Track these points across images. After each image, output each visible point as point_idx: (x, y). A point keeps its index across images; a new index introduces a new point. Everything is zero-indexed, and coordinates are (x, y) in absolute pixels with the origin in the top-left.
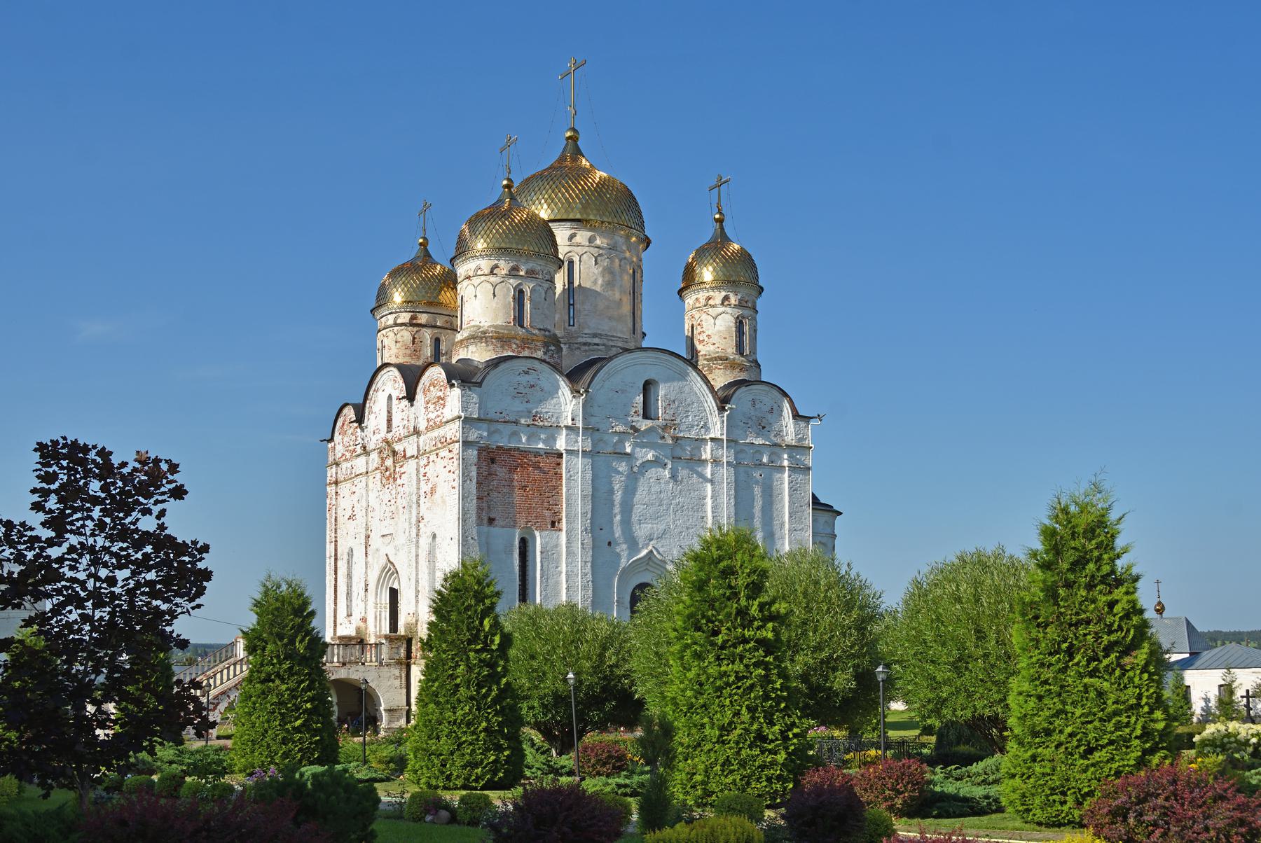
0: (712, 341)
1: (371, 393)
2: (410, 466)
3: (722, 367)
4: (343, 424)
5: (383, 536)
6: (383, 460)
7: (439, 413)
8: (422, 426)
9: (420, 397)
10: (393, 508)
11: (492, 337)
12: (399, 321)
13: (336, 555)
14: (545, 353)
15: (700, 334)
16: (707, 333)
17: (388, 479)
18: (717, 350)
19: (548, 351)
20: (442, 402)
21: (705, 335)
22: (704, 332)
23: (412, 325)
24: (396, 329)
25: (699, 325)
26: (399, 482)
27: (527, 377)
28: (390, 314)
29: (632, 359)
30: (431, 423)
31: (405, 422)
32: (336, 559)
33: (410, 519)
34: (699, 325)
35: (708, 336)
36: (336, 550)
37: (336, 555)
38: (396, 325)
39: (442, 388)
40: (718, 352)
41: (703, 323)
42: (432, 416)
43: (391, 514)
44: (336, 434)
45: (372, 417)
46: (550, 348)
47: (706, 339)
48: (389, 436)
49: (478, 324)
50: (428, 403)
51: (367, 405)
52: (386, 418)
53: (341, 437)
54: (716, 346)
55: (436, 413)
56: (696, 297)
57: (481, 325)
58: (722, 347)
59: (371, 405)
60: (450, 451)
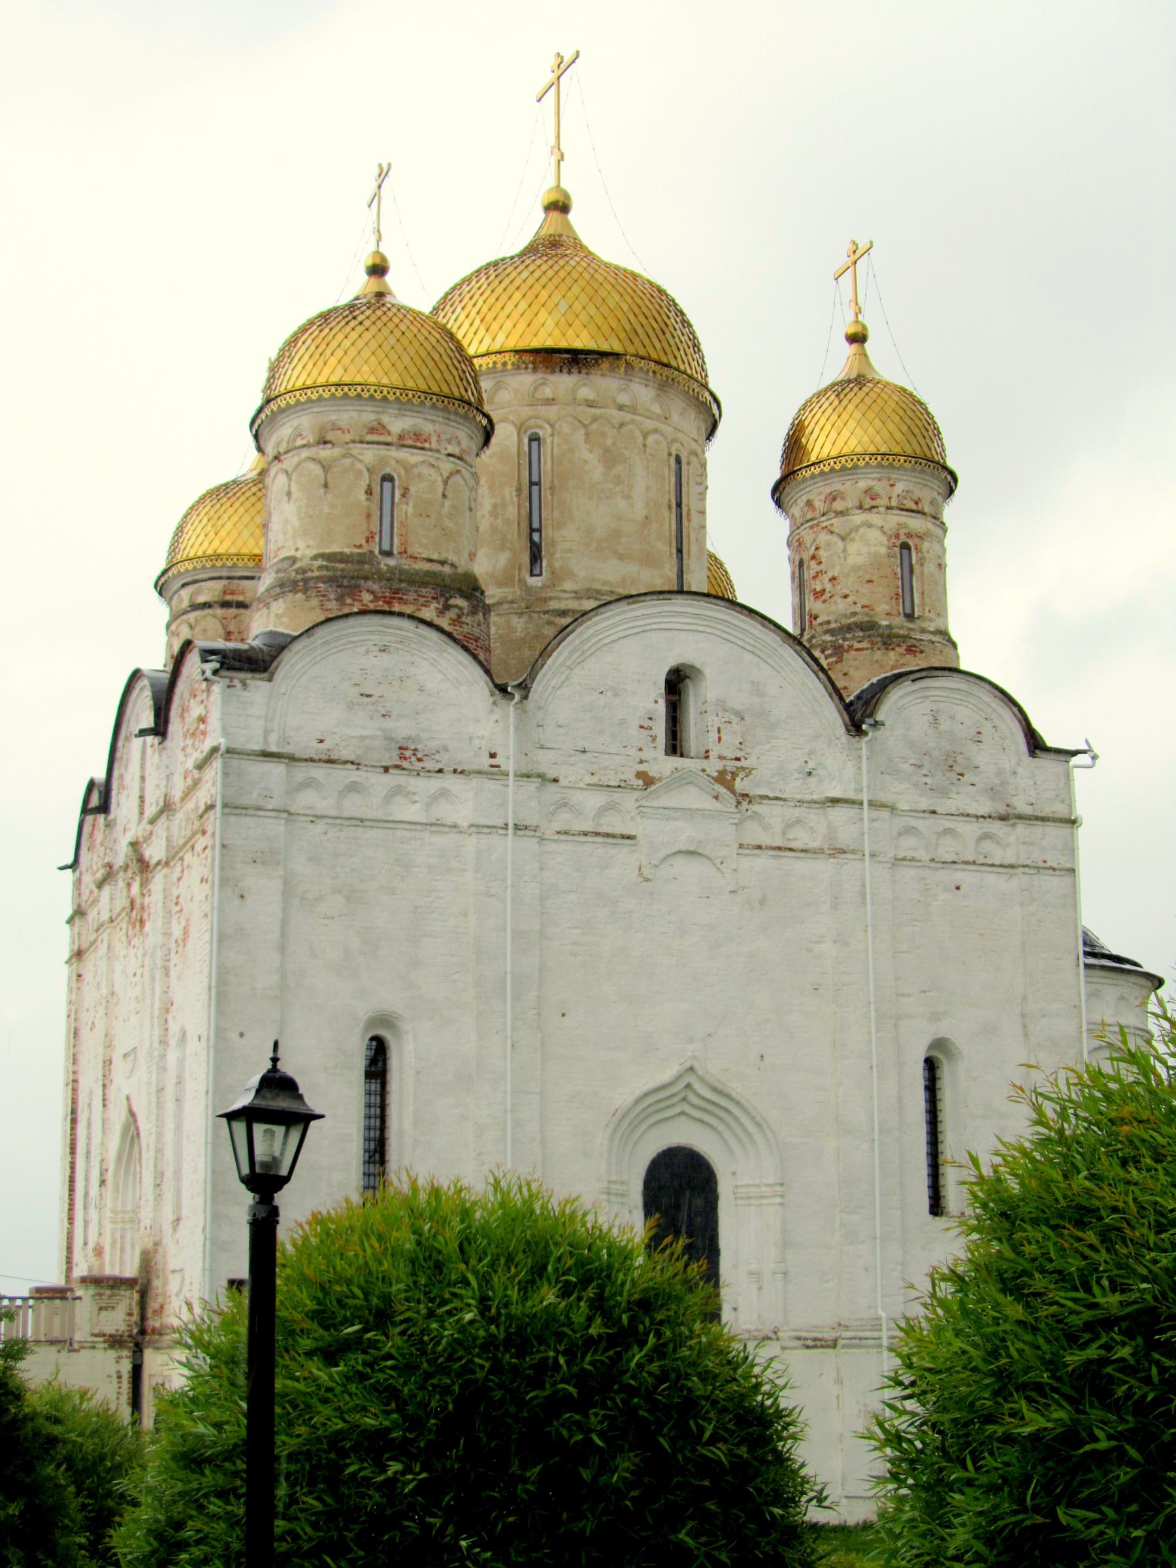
0: (841, 589)
3: (865, 644)
9: (175, 727)
11: (319, 579)
12: (201, 599)
14: (441, 613)
15: (814, 578)
16: (830, 575)
18: (852, 609)
19: (447, 607)
21: (826, 578)
23: (225, 604)
24: (192, 616)
25: (813, 557)
27: (385, 660)
29: (636, 618)
35: (833, 579)
38: (195, 607)
40: (854, 614)
41: (822, 553)
46: (452, 602)
47: (828, 586)
49: (292, 553)
54: (850, 599)
56: (805, 498)
57: (298, 555)
58: (864, 602)
59: (123, 771)
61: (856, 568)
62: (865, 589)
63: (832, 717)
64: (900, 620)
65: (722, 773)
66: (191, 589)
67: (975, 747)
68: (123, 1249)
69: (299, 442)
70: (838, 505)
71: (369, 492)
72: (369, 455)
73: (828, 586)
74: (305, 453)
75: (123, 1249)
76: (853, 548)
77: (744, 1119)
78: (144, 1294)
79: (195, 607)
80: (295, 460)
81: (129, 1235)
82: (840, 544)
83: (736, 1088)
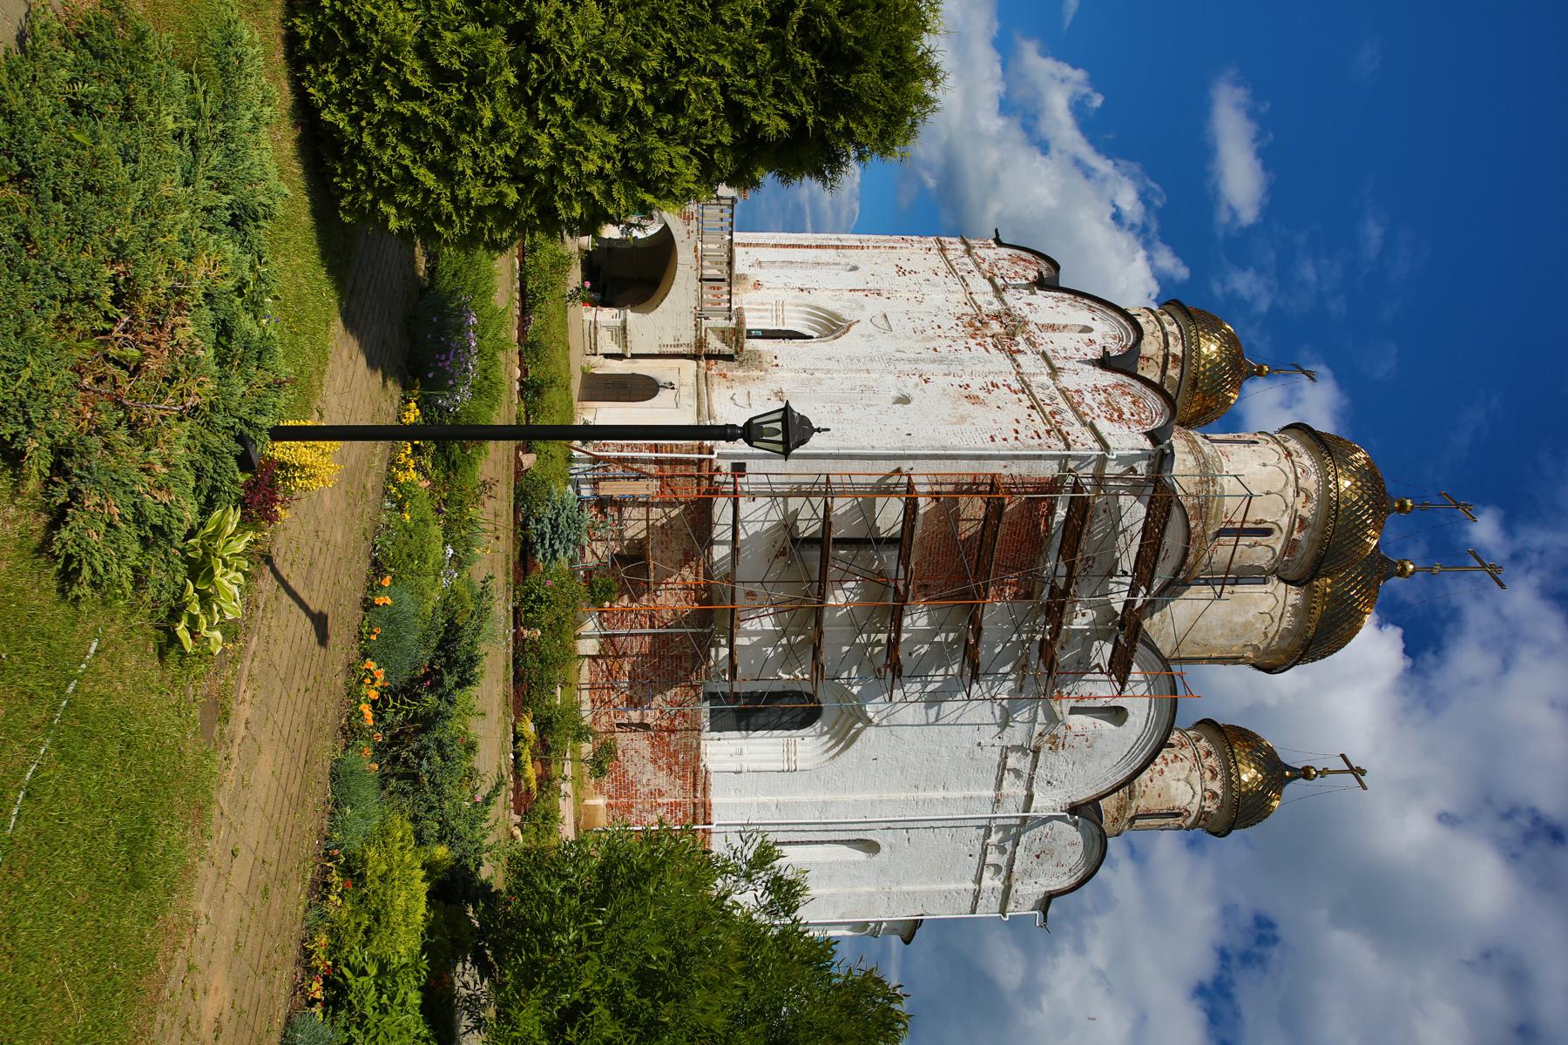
1: (1086, 301)
2: (1000, 361)
4: (1025, 260)
6: (997, 317)
7: (1097, 411)
8: (1067, 381)
9: (1108, 378)
10: (930, 333)
11: (1208, 492)
12: (1171, 339)
13: (844, 247)
17: (971, 325)
20: (1115, 416)
21: (1163, 766)
22: (1167, 764)
23: (1166, 357)
24: (1160, 334)
25: (1176, 757)
26: (972, 342)
28: (1179, 326)
30: (1077, 398)
31: (1063, 354)
32: (837, 247)
33: (923, 360)
34: (1176, 757)
35: (1162, 772)
37: (844, 247)
38: (1165, 335)
39: (1136, 417)
42: (1088, 398)
43: (920, 328)
44: (1010, 251)
45: (1050, 302)
47: (1158, 768)
48: (1032, 327)
50: (1105, 391)
51: (1066, 296)
52: (1056, 323)
53: (1006, 257)
54: (1149, 783)
55: (1095, 405)
58: (1148, 792)
59: (1068, 302)
60: (1048, 432)
61: (1168, 787)
62: (1155, 793)
63: (1083, 794)
64: (1133, 812)
65: (1056, 737)
66: (1177, 332)
67: (1054, 863)
68: (759, 310)
69: (1299, 470)
70: (1208, 775)
71: (1262, 522)
72: (1285, 521)
73: (1158, 768)
74: (1292, 477)
75: (759, 310)
76: (1182, 783)
77: (837, 749)
78: (729, 358)
79: (1165, 335)
80: (1287, 470)
81: (768, 314)
82: (1182, 777)
83: (857, 745)
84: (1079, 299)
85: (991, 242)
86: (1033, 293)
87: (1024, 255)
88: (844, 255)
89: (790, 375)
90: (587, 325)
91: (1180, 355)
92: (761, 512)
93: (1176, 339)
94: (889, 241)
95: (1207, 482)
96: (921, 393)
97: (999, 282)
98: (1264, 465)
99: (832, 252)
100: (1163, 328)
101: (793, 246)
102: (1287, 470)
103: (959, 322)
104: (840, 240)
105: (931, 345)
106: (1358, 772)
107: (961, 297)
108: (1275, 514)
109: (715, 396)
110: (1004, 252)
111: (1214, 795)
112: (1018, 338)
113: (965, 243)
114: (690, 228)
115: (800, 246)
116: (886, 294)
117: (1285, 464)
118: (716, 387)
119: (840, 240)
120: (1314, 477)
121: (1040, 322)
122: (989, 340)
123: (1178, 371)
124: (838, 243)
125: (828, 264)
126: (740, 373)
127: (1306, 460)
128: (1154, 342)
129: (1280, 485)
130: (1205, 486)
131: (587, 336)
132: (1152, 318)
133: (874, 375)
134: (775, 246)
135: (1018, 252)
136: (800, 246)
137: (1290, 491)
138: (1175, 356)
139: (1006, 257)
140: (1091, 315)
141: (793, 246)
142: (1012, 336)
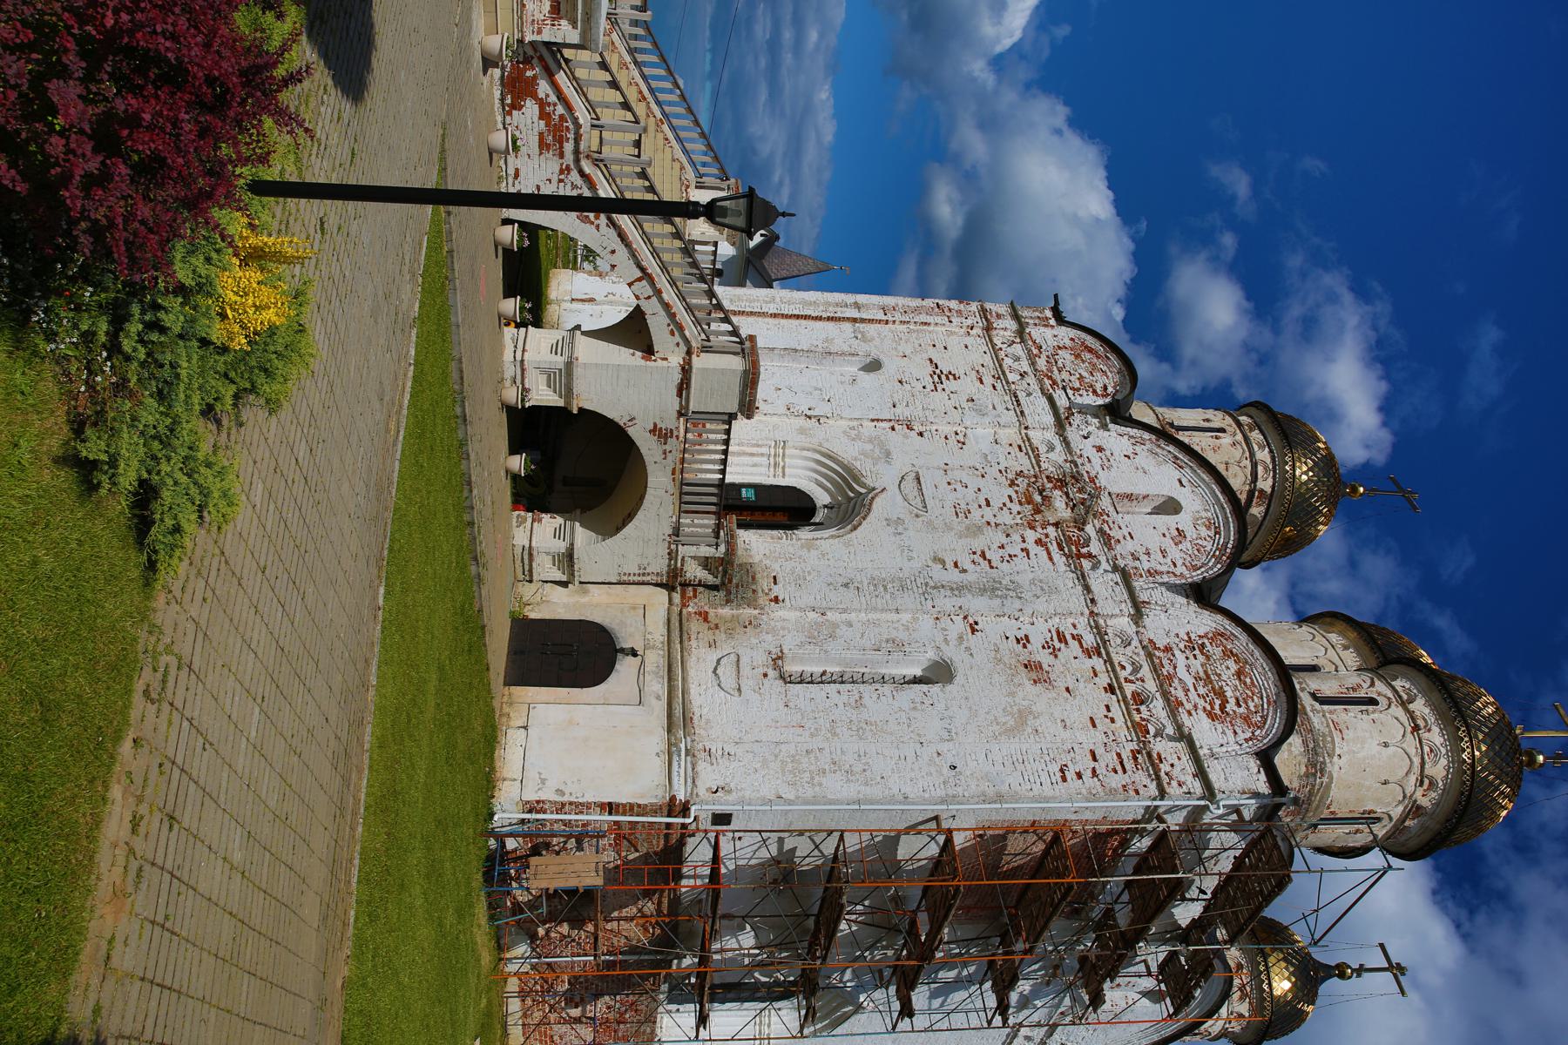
1: (1171, 448)
5: (918, 479)
12: (1260, 469)
13: (863, 321)
24: (1248, 463)
26: (1031, 536)
28: (1271, 451)
32: (855, 320)
36: (871, 321)
37: (863, 321)
38: (1254, 465)
44: (1073, 333)
48: (1105, 503)
49: (1338, 751)
51: (1147, 436)
52: (1136, 492)
53: (1068, 343)
55: (1190, 681)
57: (1336, 758)
59: (1148, 445)
66: (1268, 460)
68: (752, 455)
69: (1426, 749)
74: (1417, 761)
75: (752, 455)
79: (1254, 465)
80: (1412, 751)
84: (1162, 443)
85: (1049, 314)
86: (1104, 427)
87: (1091, 341)
88: (865, 339)
89: (792, 615)
90: (518, 551)
91: (1269, 490)
92: (749, 849)
93: (1266, 468)
94: (916, 310)
95: (1314, 775)
96: (966, 656)
97: (1062, 401)
98: (1386, 745)
99: (847, 326)
100: (1252, 455)
101: (798, 317)
102: (1412, 751)
103: (1011, 491)
104: (857, 306)
105: (978, 544)
106: (1397, 970)
107: (1011, 434)
108: (1389, 804)
109: (692, 662)
110: (1065, 334)
111: (1241, 1016)
112: (1089, 529)
113: (1016, 317)
114: (668, 447)
115: (806, 317)
116: (917, 427)
117: (1411, 744)
118: (694, 643)
119: (857, 306)
120: (1443, 762)
121: (1115, 490)
122: (1051, 530)
123: (1262, 509)
124: (856, 315)
125: (843, 354)
126: (726, 612)
127: (1436, 737)
128: (1241, 474)
129: (1402, 773)
130: (1311, 780)
131: (518, 563)
132: (1239, 437)
133: (906, 617)
134: (775, 316)
135: (1083, 335)
136: (806, 317)
137: (1413, 779)
138: (1262, 491)
139: (1068, 343)
140: (1177, 474)
141: (798, 317)
142: (1080, 524)
